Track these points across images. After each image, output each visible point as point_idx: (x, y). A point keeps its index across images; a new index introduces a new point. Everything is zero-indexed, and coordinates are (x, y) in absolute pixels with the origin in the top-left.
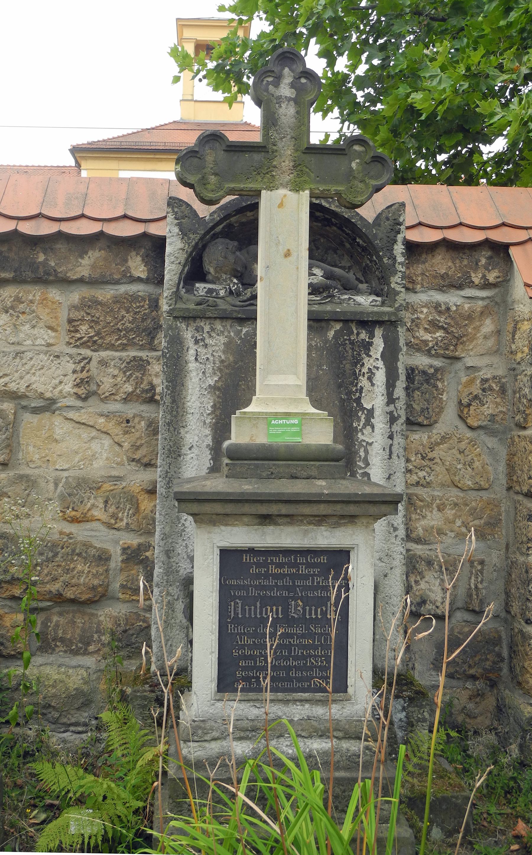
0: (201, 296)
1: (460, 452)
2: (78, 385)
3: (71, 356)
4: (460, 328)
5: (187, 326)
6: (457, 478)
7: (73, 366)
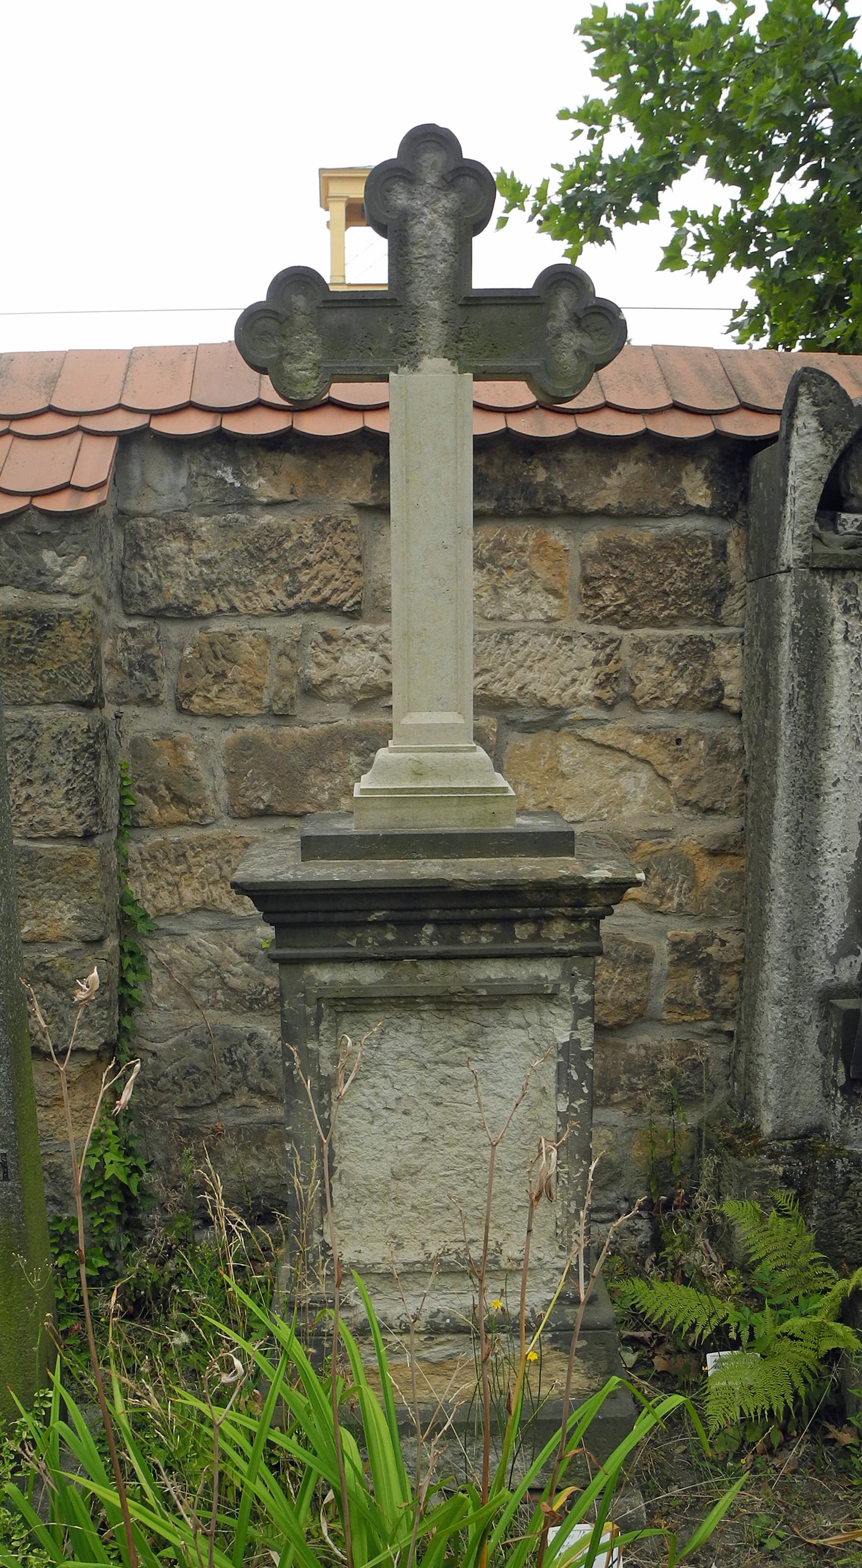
0: (849, 534)
2: (601, 685)
3: (589, 638)
5: (832, 584)
7: (594, 654)
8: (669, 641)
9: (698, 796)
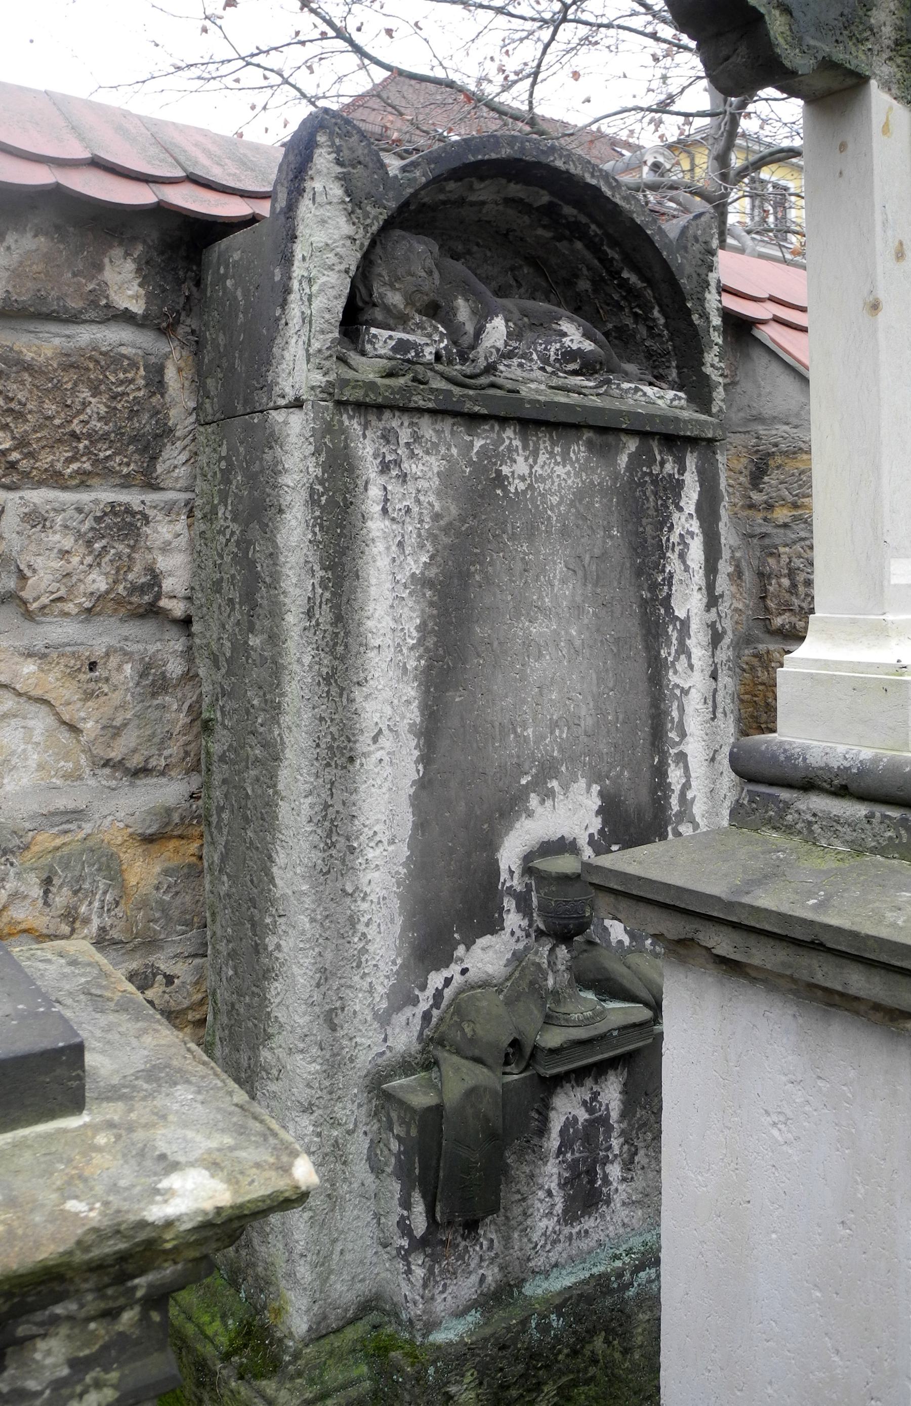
8: (79, 510)
9: (124, 750)
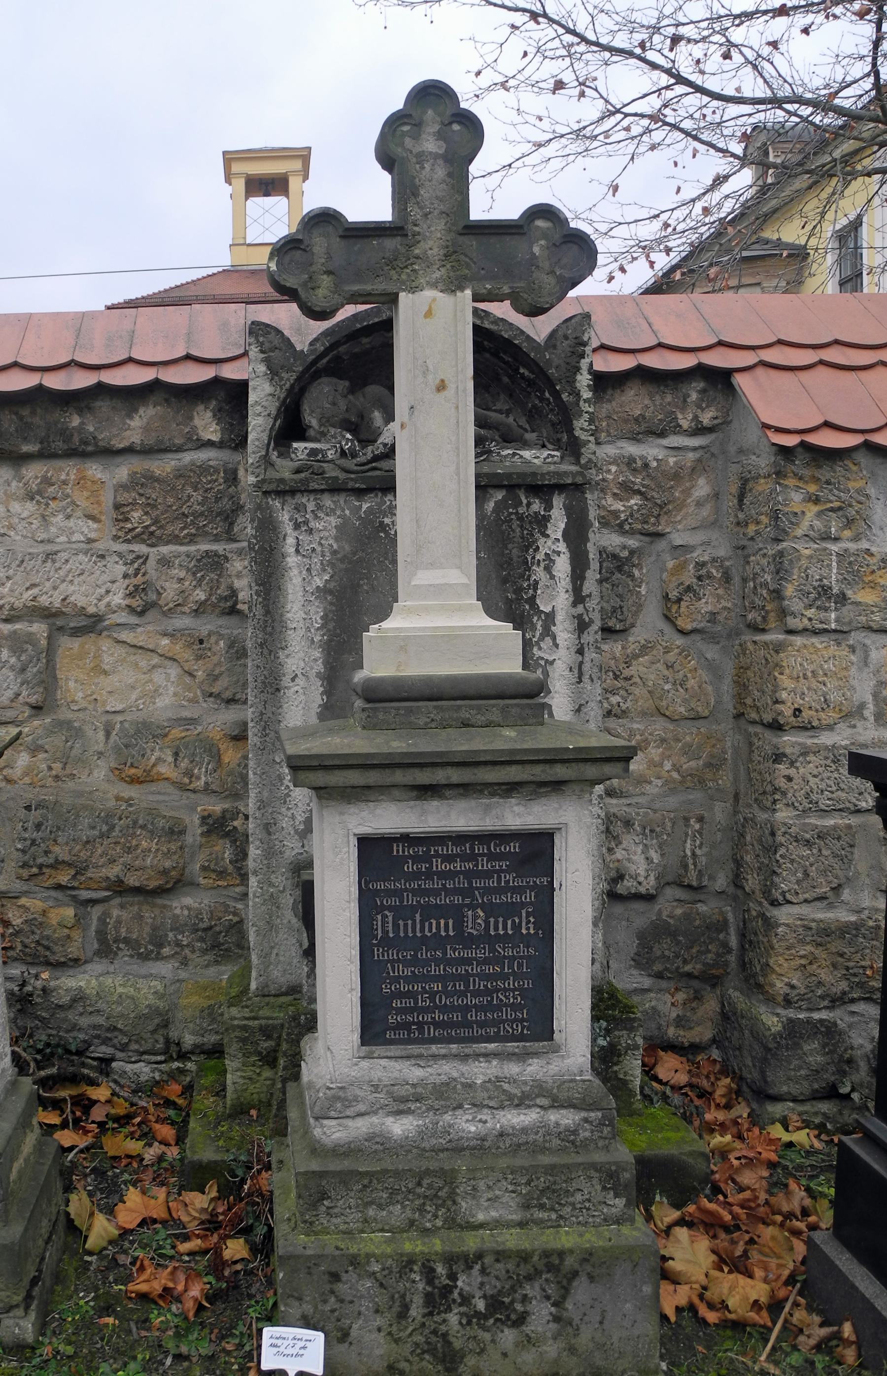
1: (668, 667)
2: (130, 595)
3: (120, 555)
4: (664, 491)
5: (283, 504)
6: (664, 703)
7: (124, 568)
8: (188, 556)
